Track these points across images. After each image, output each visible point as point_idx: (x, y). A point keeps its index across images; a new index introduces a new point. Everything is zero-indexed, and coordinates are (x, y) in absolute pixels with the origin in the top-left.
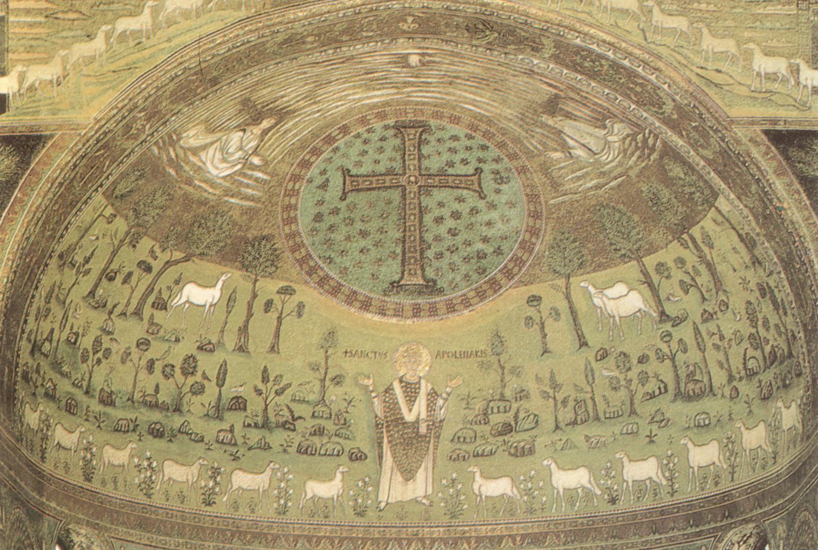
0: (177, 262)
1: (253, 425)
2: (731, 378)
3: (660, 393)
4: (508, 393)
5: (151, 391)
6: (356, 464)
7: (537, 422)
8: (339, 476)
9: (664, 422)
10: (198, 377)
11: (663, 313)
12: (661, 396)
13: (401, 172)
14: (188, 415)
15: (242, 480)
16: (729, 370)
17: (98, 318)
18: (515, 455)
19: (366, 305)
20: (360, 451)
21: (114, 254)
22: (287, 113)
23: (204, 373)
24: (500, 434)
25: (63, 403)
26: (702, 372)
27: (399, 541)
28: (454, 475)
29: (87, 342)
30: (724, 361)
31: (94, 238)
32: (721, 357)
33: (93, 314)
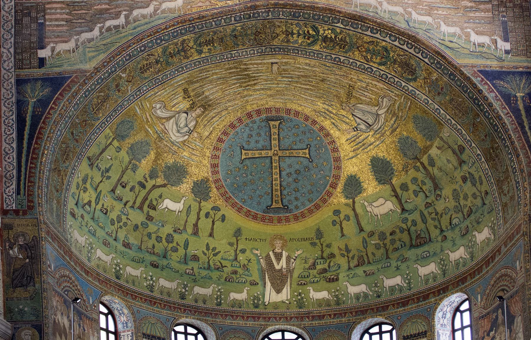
1: (203, 268)
3: (402, 247)
5: (150, 246)
6: (253, 287)
7: (339, 267)
12: (402, 248)
14: (171, 260)
17: (119, 206)
20: (255, 281)
24: (322, 273)
26: (425, 233)
28: (300, 291)
30: (438, 224)
31: (110, 158)
32: (437, 223)
33: (115, 203)
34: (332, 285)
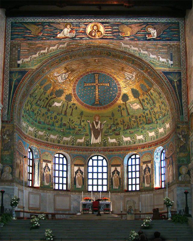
0: (53, 98)
2: (156, 120)
4: (115, 124)
8: (83, 138)
9: (144, 128)
10: (57, 120)
11: (143, 109)
13: (94, 82)
15: (65, 139)
16: (156, 118)
17: (38, 108)
18: (116, 135)
19: (88, 107)
21: (41, 96)
22: (73, 71)
23: (58, 119)
25: (31, 123)
27: (95, 150)
29: (36, 112)
30: (155, 116)
33: (37, 107)
34: (117, 136)
